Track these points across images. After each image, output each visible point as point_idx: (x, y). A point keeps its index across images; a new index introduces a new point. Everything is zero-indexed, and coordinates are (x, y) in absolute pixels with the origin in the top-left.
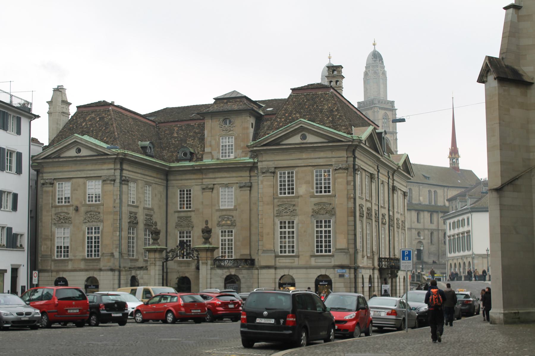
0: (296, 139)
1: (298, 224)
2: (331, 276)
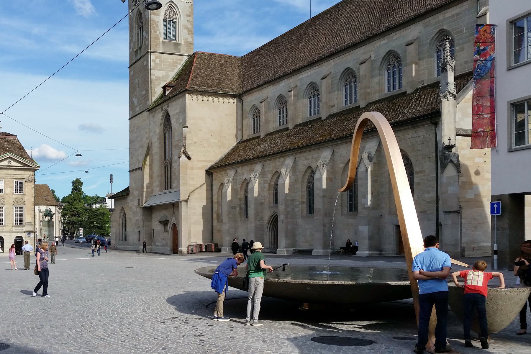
0: (5, 163)
1: (5, 209)
2: (23, 237)
